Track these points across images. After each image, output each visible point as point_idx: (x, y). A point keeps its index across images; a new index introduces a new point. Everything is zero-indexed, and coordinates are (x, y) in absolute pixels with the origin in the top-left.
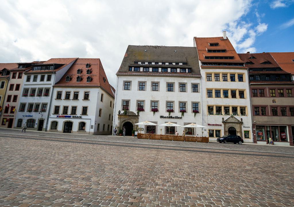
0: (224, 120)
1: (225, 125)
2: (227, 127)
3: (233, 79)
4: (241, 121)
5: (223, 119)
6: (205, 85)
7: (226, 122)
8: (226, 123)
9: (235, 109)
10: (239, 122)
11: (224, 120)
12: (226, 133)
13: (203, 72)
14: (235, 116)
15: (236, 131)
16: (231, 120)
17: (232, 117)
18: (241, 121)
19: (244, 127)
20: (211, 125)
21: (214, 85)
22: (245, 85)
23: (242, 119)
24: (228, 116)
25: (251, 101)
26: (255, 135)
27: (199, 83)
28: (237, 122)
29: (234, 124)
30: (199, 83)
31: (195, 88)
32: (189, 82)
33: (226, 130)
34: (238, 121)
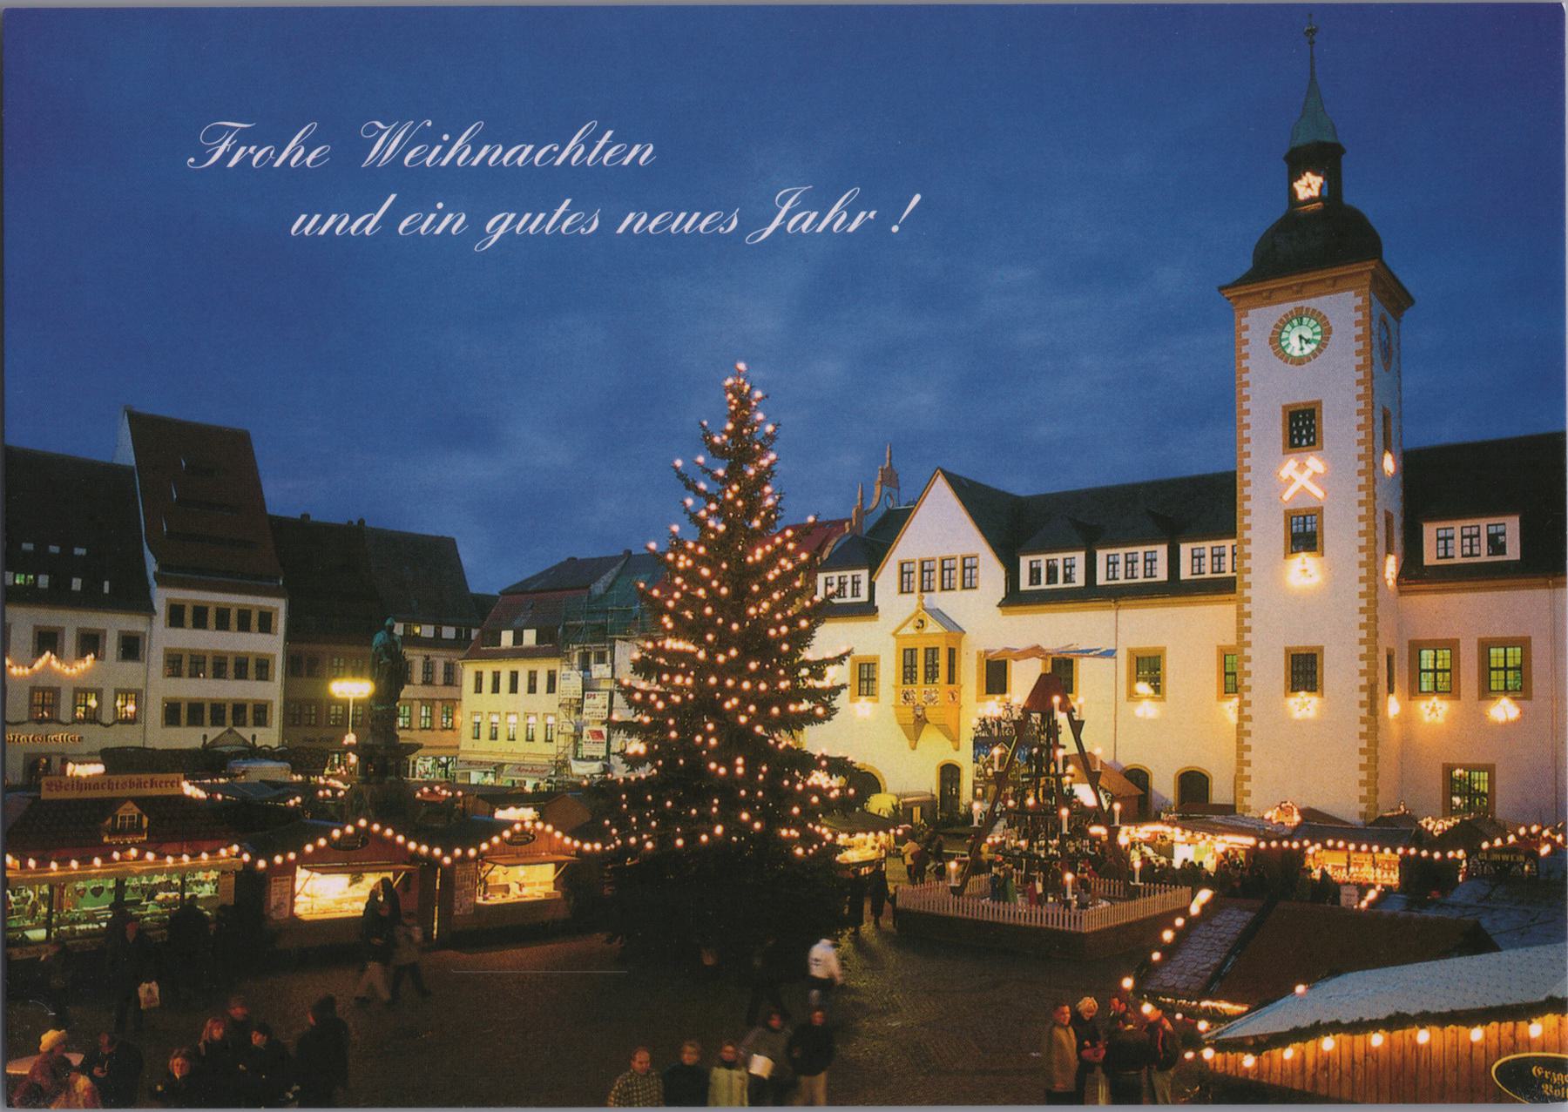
3: (244, 626)
5: (205, 737)
6: (162, 637)
9: (239, 708)
11: (208, 742)
13: (162, 597)
14: (236, 729)
17: (230, 731)
21: (189, 639)
22: (273, 645)
23: (254, 737)
24: (220, 730)
25: (287, 689)
31: (131, 648)
32: (114, 624)
34: (245, 741)
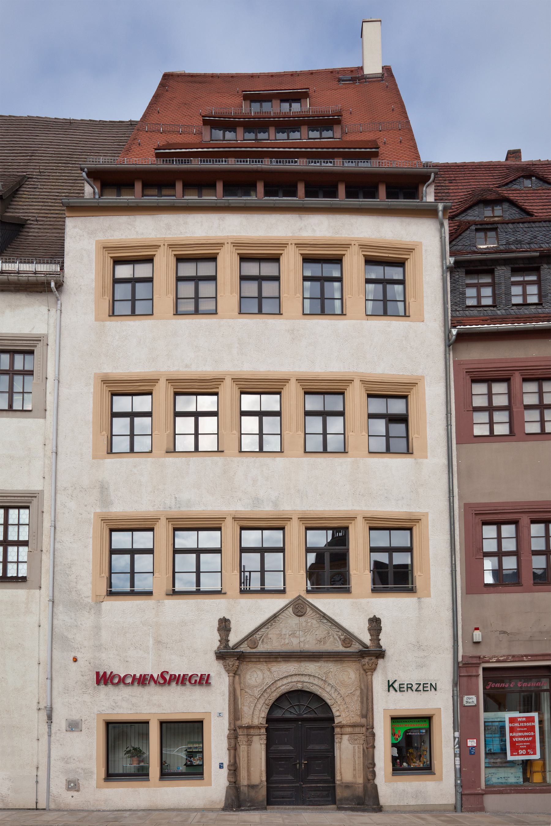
0: (233, 639)
1: (235, 673)
2: (257, 693)
4: (366, 638)
7: (244, 648)
8: (242, 657)
10: (355, 647)
12: (242, 739)
15: (332, 719)
16: (293, 634)
18: (366, 638)
19: (390, 686)
20: (122, 680)
26: (471, 743)
27: (46, 336)
28: (340, 648)
29: (311, 667)
30: (46, 336)
33: (246, 721)
